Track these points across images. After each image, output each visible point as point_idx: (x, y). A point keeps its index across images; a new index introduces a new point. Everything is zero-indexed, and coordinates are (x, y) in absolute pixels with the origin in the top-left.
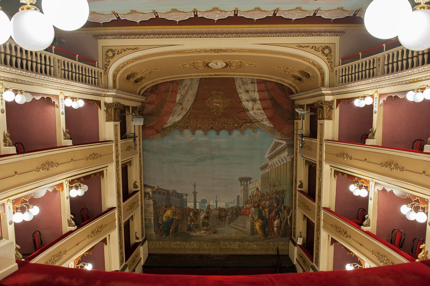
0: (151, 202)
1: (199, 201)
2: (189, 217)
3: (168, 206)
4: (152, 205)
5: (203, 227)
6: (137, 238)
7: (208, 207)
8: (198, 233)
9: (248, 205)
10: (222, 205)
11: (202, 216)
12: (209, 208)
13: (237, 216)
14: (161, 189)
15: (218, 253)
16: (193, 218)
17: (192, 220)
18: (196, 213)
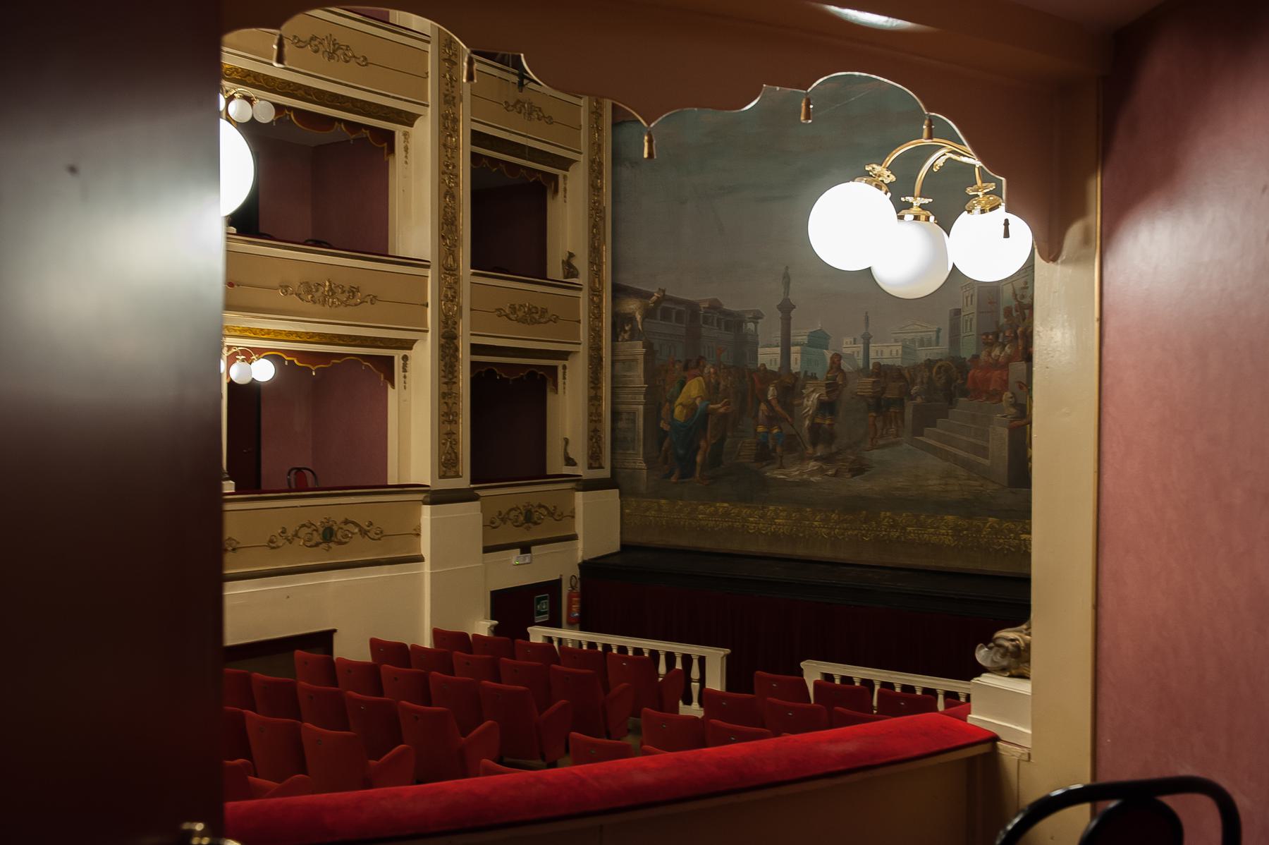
0: (639, 348)
1: (799, 339)
2: (763, 407)
3: (693, 365)
4: (641, 358)
5: (814, 445)
6: (570, 462)
7: (833, 362)
8: (794, 472)
9: (996, 352)
10: (886, 355)
11: (811, 399)
12: (839, 369)
13: (950, 399)
14: (671, 300)
15: (869, 556)
16: (778, 409)
17: (772, 419)
18: (790, 386)
